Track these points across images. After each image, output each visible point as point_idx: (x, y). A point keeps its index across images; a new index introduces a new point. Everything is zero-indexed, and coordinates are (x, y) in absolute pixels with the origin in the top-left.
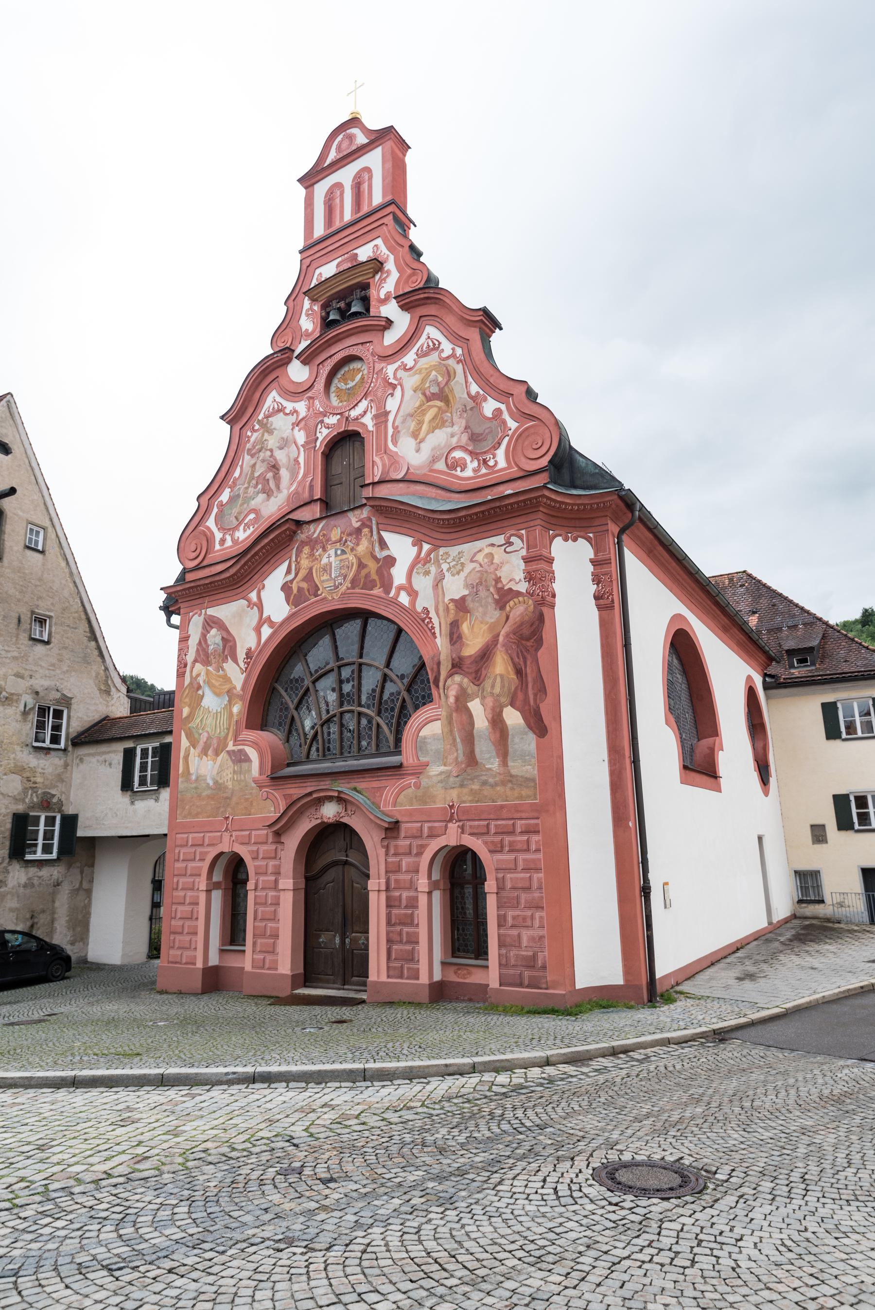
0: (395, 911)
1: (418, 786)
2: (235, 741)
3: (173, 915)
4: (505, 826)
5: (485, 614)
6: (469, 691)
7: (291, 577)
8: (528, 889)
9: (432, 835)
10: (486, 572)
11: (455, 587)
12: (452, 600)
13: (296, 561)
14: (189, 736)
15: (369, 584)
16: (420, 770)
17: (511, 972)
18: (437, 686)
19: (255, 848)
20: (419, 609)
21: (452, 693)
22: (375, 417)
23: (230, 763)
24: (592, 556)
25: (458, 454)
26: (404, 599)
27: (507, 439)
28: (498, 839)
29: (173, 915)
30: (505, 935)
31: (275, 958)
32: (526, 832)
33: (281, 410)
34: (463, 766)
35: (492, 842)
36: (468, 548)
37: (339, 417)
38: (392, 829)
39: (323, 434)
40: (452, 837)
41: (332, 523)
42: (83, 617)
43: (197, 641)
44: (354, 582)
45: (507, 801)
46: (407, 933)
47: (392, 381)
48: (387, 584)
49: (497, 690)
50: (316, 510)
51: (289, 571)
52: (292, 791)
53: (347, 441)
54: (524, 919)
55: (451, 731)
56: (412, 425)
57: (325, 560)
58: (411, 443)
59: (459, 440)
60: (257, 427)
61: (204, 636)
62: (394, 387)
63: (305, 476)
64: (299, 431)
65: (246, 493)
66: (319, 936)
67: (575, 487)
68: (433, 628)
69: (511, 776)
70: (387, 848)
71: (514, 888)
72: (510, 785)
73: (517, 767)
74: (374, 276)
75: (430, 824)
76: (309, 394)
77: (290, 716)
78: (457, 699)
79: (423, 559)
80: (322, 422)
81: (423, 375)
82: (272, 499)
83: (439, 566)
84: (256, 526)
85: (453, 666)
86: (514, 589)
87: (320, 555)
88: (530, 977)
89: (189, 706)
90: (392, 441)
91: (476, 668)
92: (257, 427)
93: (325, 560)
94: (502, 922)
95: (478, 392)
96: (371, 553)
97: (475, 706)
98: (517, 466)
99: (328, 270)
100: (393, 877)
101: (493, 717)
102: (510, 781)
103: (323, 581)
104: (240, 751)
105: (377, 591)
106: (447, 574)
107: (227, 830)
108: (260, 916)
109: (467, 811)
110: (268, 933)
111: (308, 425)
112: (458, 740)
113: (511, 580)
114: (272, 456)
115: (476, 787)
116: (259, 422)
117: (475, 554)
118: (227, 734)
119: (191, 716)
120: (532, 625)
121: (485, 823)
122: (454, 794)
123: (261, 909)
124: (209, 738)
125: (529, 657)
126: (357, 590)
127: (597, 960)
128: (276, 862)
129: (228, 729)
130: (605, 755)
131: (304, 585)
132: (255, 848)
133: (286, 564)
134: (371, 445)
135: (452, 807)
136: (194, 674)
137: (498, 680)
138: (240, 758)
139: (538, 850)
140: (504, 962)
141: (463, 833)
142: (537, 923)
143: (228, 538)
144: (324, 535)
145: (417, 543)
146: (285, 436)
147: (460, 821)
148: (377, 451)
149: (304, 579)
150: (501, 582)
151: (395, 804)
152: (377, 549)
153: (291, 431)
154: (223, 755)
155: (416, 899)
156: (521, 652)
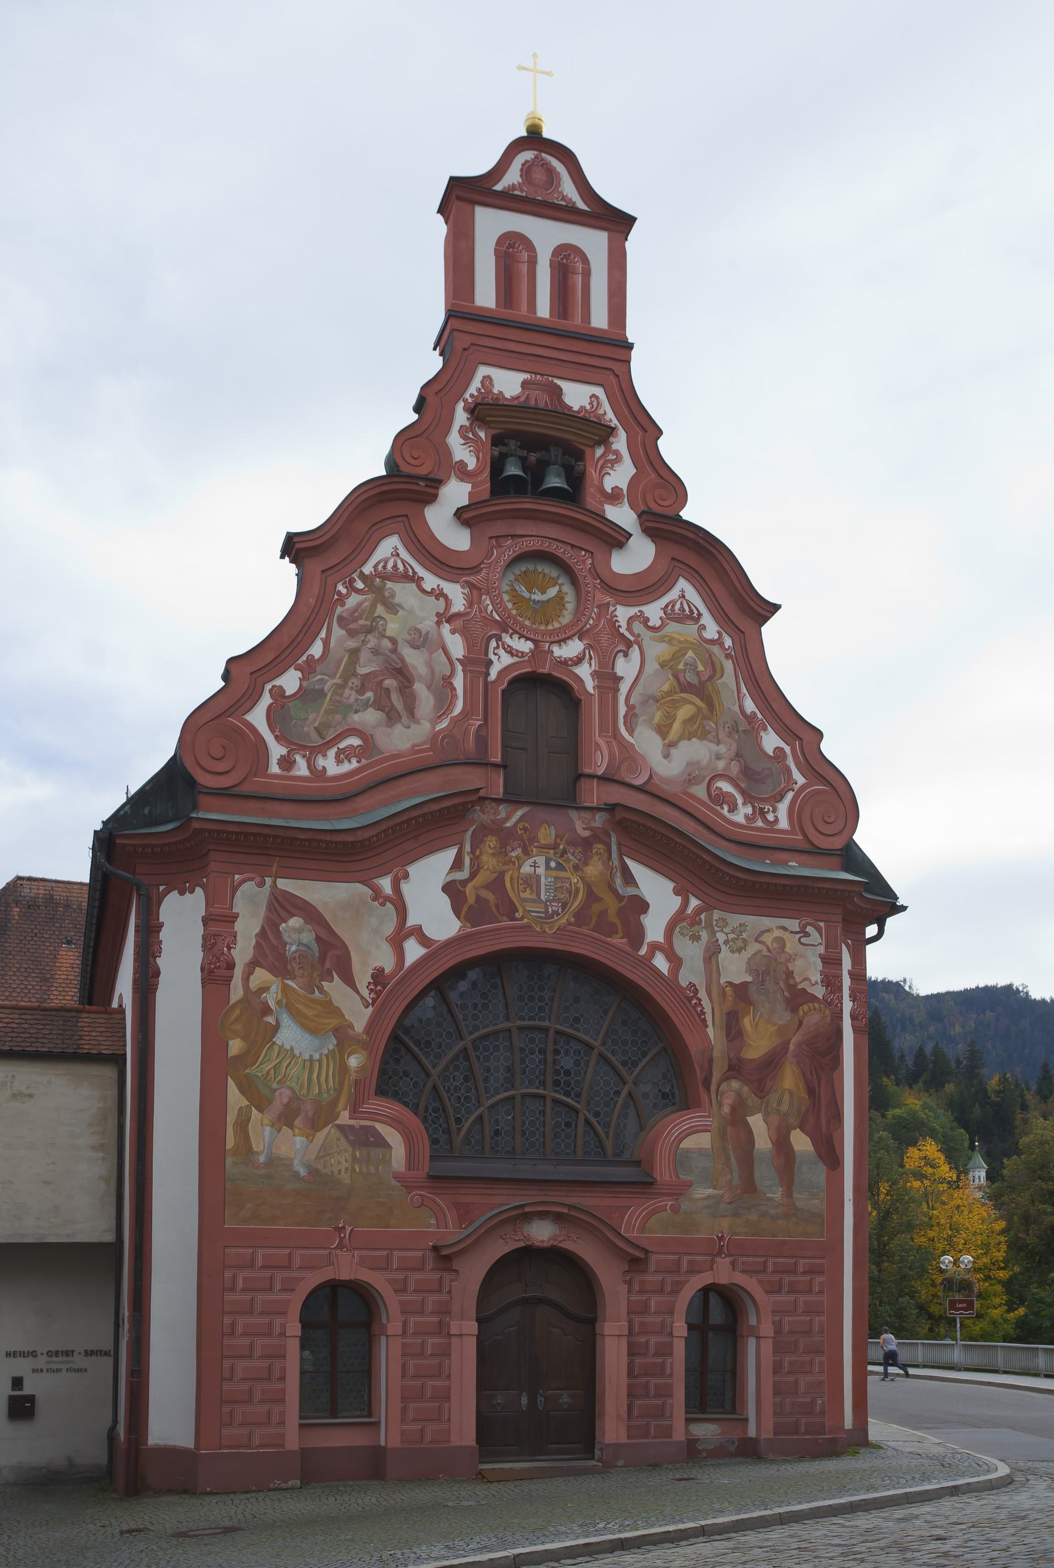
0: (638, 1360)
1: (676, 1209)
6: (750, 1102)
7: (464, 875)
9: (693, 1270)
10: (776, 960)
11: (734, 968)
12: (730, 983)
13: (473, 852)
14: (247, 1088)
15: (605, 927)
16: (679, 1190)
18: (708, 1089)
19: (400, 1276)
21: (728, 1101)
22: (595, 674)
23: (344, 1144)
25: (726, 787)
26: (661, 963)
27: (790, 795)
28: (776, 1277)
32: (812, 1271)
33: (418, 581)
38: (636, 1262)
39: (500, 661)
40: (723, 1274)
43: (257, 930)
44: (581, 917)
46: (656, 1385)
47: (622, 630)
48: (637, 935)
49: (785, 1107)
51: (457, 864)
56: (658, 716)
57: (526, 869)
59: (728, 767)
60: (360, 585)
62: (629, 644)
64: (453, 632)
65: (341, 695)
68: (704, 1013)
70: (630, 1283)
73: (801, 1198)
74: (593, 447)
75: (691, 1258)
77: (429, 1085)
78: (733, 1109)
79: (689, 916)
80: (499, 638)
81: (675, 649)
82: (398, 728)
83: (713, 933)
84: (364, 761)
85: (731, 1068)
89: (244, 1038)
90: (625, 724)
93: (526, 869)
94: (777, 1368)
95: (753, 713)
96: (609, 883)
97: (756, 1122)
100: (637, 1320)
103: (525, 900)
106: (723, 947)
107: (340, 1246)
108: (411, 1371)
111: (479, 634)
112: (733, 1160)
113: (805, 980)
114: (394, 651)
115: (753, 1217)
116: (363, 577)
117: (762, 933)
119: (247, 1057)
121: (762, 1260)
122: (725, 1224)
123: (412, 1363)
124: (295, 1098)
126: (584, 930)
128: (443, 1297)
129: (339, 1091)
131: (491, 897)
132: (400, 1276)
134: (593, 713)
135: (721, 1239)
136: (254, 983)
137: (787, 1096)
139: (821, 1292)
142: (816, 1368)
144: (525, 829)
147: (730, 1256)
151: (642, 1229)
152: (618, 880)
155: (671, 1344)
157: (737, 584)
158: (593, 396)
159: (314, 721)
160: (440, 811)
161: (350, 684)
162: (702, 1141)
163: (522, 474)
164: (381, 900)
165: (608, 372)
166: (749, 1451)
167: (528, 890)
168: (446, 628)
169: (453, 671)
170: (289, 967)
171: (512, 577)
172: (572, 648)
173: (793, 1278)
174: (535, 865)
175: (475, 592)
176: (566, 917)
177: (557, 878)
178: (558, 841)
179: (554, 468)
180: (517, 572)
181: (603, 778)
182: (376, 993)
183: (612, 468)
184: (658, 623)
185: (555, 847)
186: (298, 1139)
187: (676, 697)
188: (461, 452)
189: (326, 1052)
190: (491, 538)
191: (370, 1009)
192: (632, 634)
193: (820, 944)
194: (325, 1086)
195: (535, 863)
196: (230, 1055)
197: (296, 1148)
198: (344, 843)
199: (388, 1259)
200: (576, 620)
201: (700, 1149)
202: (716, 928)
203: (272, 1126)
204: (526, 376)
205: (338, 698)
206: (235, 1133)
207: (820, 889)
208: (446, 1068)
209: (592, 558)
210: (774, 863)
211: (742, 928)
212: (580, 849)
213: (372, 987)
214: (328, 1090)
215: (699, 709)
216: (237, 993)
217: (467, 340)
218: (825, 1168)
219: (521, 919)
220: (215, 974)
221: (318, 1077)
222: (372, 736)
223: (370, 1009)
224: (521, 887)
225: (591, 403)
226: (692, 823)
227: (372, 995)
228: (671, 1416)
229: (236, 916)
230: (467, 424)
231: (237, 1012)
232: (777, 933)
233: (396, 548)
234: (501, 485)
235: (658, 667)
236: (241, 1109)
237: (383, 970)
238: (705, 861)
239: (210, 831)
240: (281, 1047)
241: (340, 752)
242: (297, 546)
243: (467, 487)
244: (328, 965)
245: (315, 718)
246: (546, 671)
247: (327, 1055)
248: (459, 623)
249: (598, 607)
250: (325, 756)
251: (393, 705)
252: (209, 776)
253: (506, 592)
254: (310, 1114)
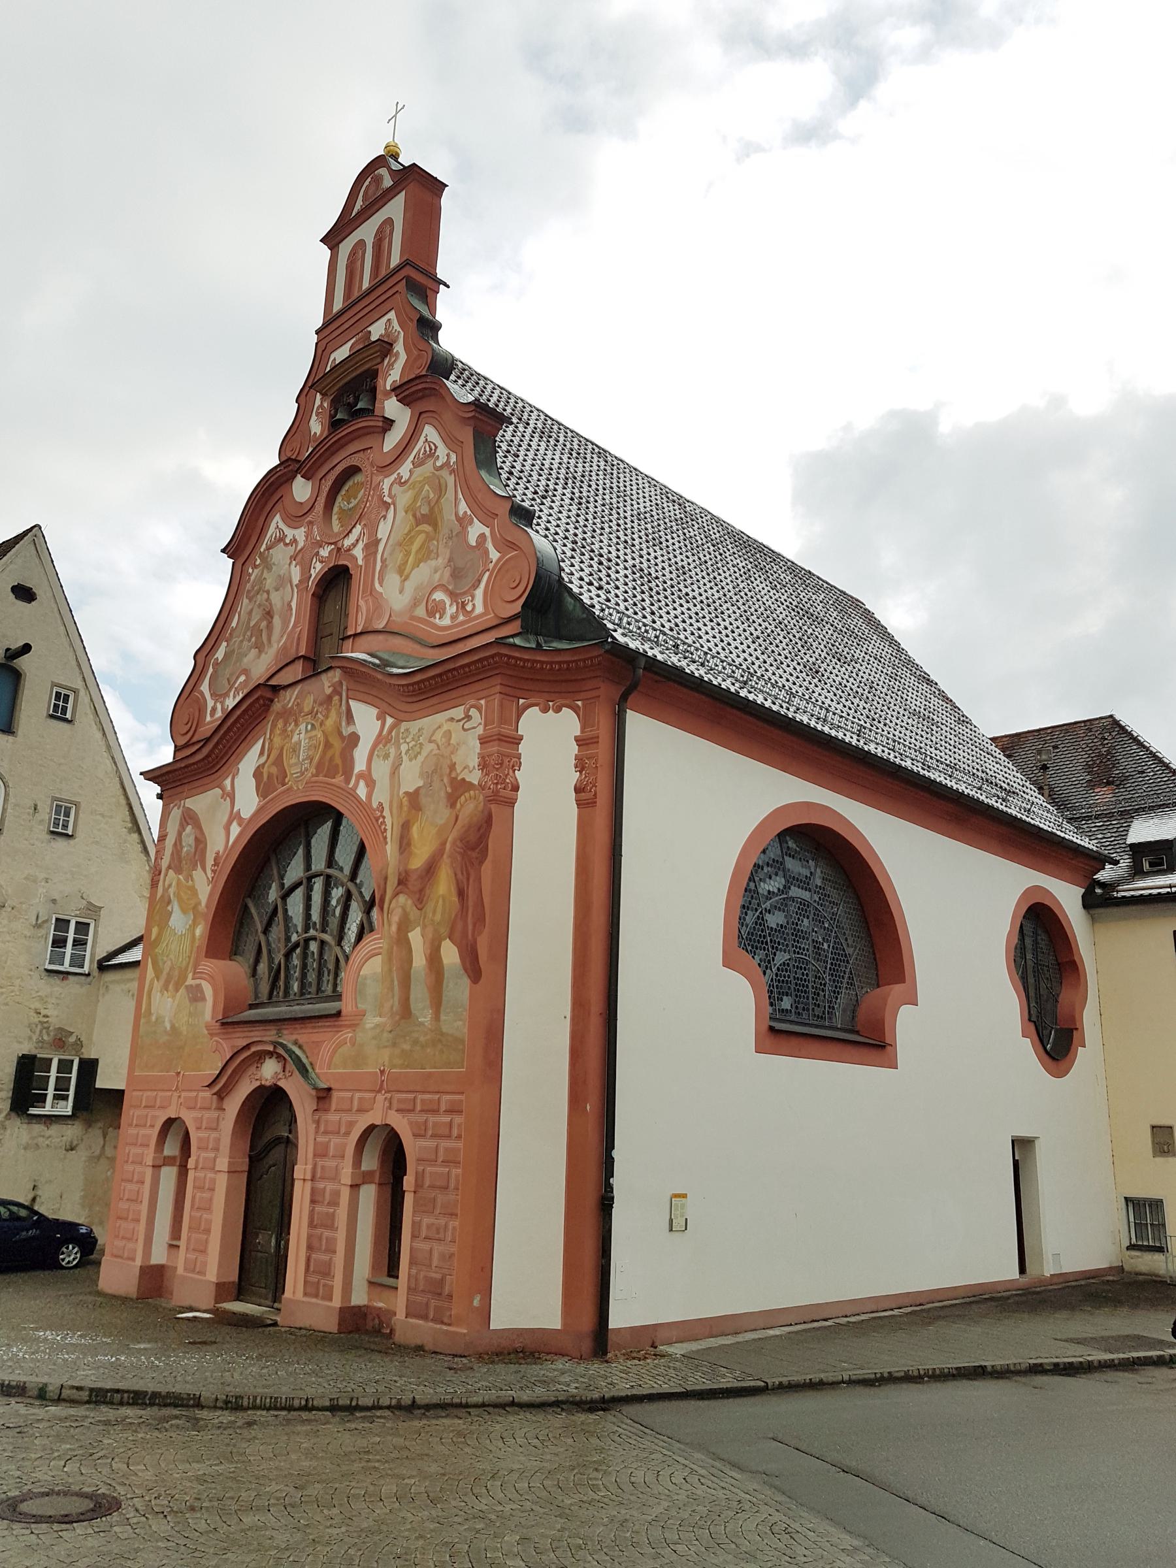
0: (318, 1208)
2: (195, 973)
4: (431, 1101)
6: (412, 917)
22: (366, 547)
24: (578, 733)
25: (439, 596)
26: (362, 791)
42: (123, 802)
44: (319, 767)
47: (387, 499)
49: (438, 917)
50: (296, 671)
51: (262, 753)
57: (295, 738)
61: (180, 834)
62: (387, 506)
67: (560, 638)
68: (385, 830)
69: (442, 1034)
70: (318, 1122)
71: (432, 1187)
72: (440, 1046)
74: (383, 361)
78: (399, 929)
80: (317, 554)
83: (398, 747)
85: (400, 882)
92: (258, 562)
97: (416, 937)
102: (440, 1041)
105: (339, 780)
106: (405, 758)
111: (302, 558)
112: (396, 983)
114: (268, 599)
115: (407, 1047)
120: (479, 830)
121: (411, 1096)
125: (472, 872)
126: (321, 778)
127: (527, 1290)
130: (567, 1010)
135: (382, 1072)
138: (196, 995)
140: (413, 1286)
141: (390, 1108)
143: (219, 706)
145: (381, 717)
146: (282, 573)
147: (388, 1092)
153: (289, 571)
154: (182, 991)
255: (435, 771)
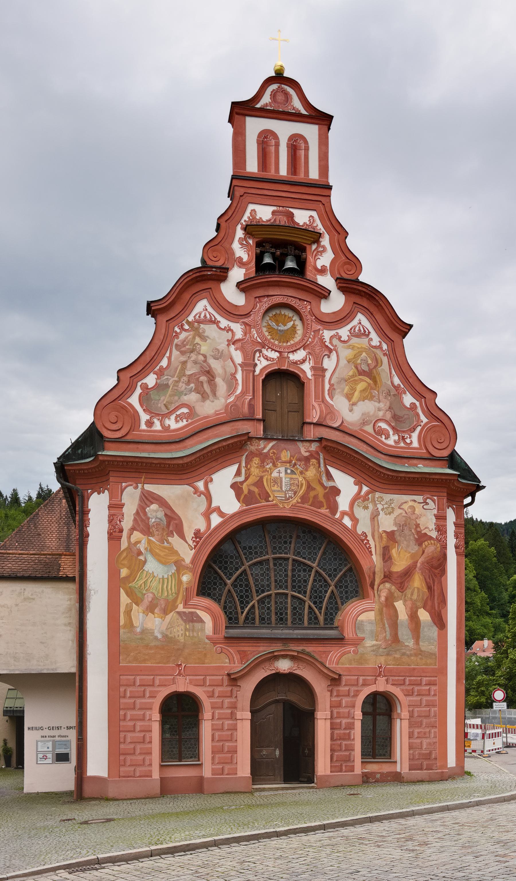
0: (336, 732)
1: (356, 652)
3: (122, 740)
4: (415, 680)
5: (408, 546)
6: (396, 595)
7: (242, 479)
8: (428, 716)
10: (410, 518)
11: (387, 523)
12: (385, 531)
13: (246, 466)
14: (130, 593)
16: (358, 642)
17: (416, 762)
18: (373, 588)
19: (210, 689)
20: (360, 532)
22: (313, 368)
23: (180, 621)
25: (383, 425)
26: (347, 522)
27: (419, 428)
28: (411, 687)
29: (122, 740)
30: (413, 743)
31: (233, 766)
32: (429, 684)
34: (390, 642)
35: (406, 690)
36: (398, 498)
37: (277, 354)
38: (335, 680)
39: (261, 364)
40: (381, 686)
41: (282, 445)
43: (135, 512)
44: (304, 499)
45: (417, 666)
46: (345, 745)
48: (333, 507)
49: (415, 597)
51: (238, 473)
52: (246, 649)
53: (282, 378)
54: (425, 733)
55: (382, 619)
56: (347, 389)
57: (275, 474)
58: (346, 401)
59: (384, 415)
60: (186, 327)
62: (330, 351)
63: (243, 393)
64: (236, 349)
66: (262, 751)
69: (421, 651)
70: (331, 692)
71: (419, 716)
73: (424, 646)
74: (310, 244)
75: (364, 678)
76: (246, 320)
78: (387, 599)
80: (260, 351)
81: (355, 352)
82: (208, 402)
83: (375, 505)
84: (190, 421)
85: (385, 577)
86: (429, 534)
87: (270, 469)
88: (427, 764)
90: (328, 394)
91: (401, 581)
92: (186, 327)
93: (275, 474)
94: (411, 736)
96: (319, 480)
97: (399, 605)
98: (427, 449)
99: (264, 213)
100: (335, 711)
101: (411, 614)
102: (420, 654)
103: (273, 491)
104: (192, 613)
105: (324, 511)
106: (381, 512)
108: (217, 738)
109: (390, 670)
110: (226, 750)
111: (250, 349)
112: (387, 625)
113: (426, 528)
114: (205, 361)
115: (397, 656)
116: (188, 323)
117: (402, 504)
118: (177, 598)
120: (439, 560)
121: (403, 678)
122: (382, 660)
123: (217, 734)
124: (154, 598)
125: (436, 579)
126: (306, 506)
128: (233, 700)
131: (256, 490)
132: (210, 689)
133: (235, 467)
134: (311, 389)
135: (380, 667)
136: (133, 539)
137: (416, 590)
139: (435, 695)
140: (411, 757)
142: (432, 735)
144: (274, 453)
147: (385, 676)
148: (315, 398)
149: (256, 484)
150: (420, 527)
151: (337, 663)
152: (324, 478)
155: (354, 722)
156: (432, 576)
157: (389, 315)
158: (311, 216)
159: (164, 400)
160: (228, 445)
161: (182, 380)
162: (371, 616)
163: (273, 262)
164: (198, 494)
165: (318, 203)
166: (397, 778)
167: (276, 486)
168: (232, 347)
169: (236, 371)
170: (151, 530)
171: (268, 318)
172: (300, 355)
173: (419, 688)
174: (279, 472)
175: (248, 327)
176: (296, 499)
177: (291, 479)
178: (292, 458)
179: (289, 257)
180: (271, 315)
181: (316, 424)
182: (196, 542)
183: (321, 255)
184: (346, 338)
185: (290, 462)
186: (157, 619)
187: (356, 378)
188: (240, 251)
189: (170, 574)
190: (256, 298)
191: (194, 551)
192: (332, 345)
193: (434, 508)
194: (170, 592)
195: (279, 471)
196: (121, 577)
197: (156, 624)
198: (178, 465)
199: (204, 680)
200: (303, 339)
201: (369, 620)
202: (377, 502)
203: (144, 613)
204: (275, 208)
205: (176, 388)
206: (125, 617)
207: (433, 479)
208: (236, 580)
209: (310, 305)
210: (411, 465)
211: (392, 502)
212: (303, 463)
213: (194, 539)
214: (172, 594)
215: (369, 384)
216: (124, 544)
217: (241, 191)
218: (437, 629)
219: (272, 501)
220: (114, 535)
221: (167, 587)
222: (194, 407)
223: (194, 551)
224: (272, 484)
225: (310, 221)
226: (365, 446)
227: (194, 544)
228: (354, 761)
229: (123, 505)
230: (243, 236)
231: (125, 554)
232: (411, 504)
233: (205, 306)
234: (261, 268)
235: (346, 362)
236: (127, 604)
237: (200, 530)
238: (370, 466)
239: (108, 461)
240: (147, 572)
241: (177, 416)
242: (153, 308)
243: (243, 271)
244: (171, 528)
245: (164, 399)
246: (285, 368)
247: (171, 576)
248: (239, 344)
249: (314, 331)
250: (169, 419)
251: (205, 391)
252: (109, 432)
253: (265, 326)
254: (163, 606)
255: (405, 525)
